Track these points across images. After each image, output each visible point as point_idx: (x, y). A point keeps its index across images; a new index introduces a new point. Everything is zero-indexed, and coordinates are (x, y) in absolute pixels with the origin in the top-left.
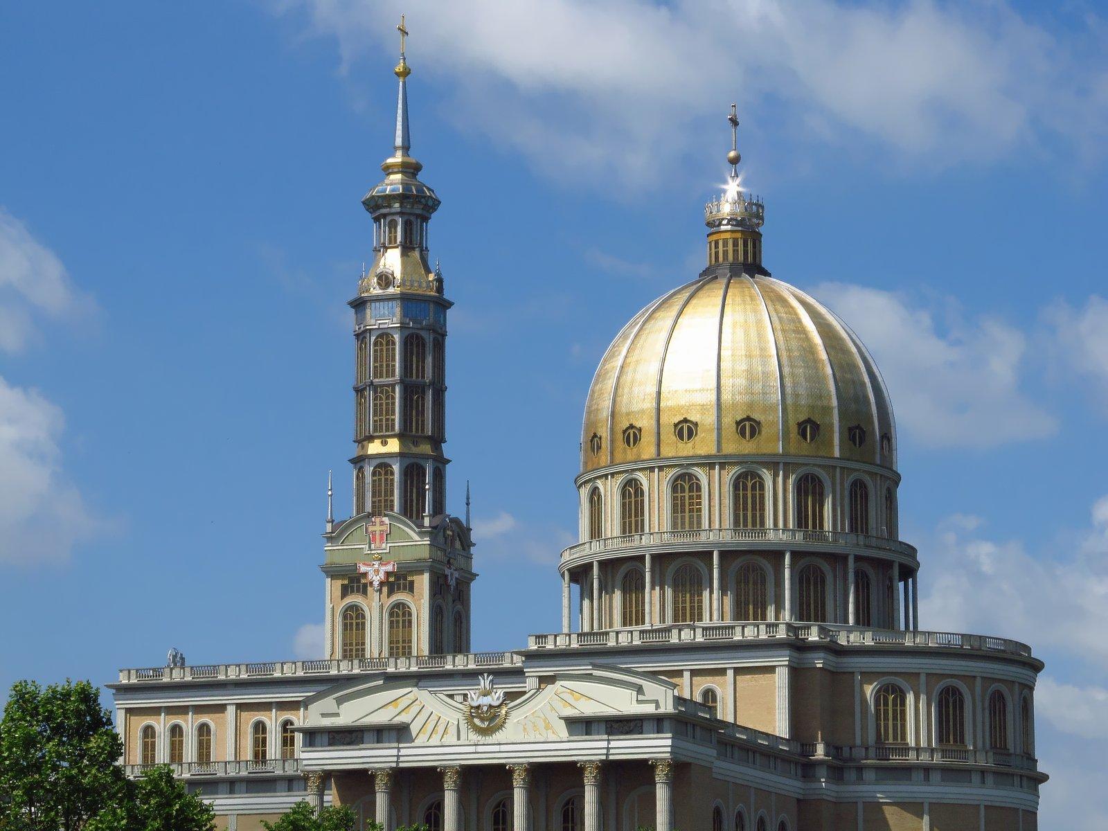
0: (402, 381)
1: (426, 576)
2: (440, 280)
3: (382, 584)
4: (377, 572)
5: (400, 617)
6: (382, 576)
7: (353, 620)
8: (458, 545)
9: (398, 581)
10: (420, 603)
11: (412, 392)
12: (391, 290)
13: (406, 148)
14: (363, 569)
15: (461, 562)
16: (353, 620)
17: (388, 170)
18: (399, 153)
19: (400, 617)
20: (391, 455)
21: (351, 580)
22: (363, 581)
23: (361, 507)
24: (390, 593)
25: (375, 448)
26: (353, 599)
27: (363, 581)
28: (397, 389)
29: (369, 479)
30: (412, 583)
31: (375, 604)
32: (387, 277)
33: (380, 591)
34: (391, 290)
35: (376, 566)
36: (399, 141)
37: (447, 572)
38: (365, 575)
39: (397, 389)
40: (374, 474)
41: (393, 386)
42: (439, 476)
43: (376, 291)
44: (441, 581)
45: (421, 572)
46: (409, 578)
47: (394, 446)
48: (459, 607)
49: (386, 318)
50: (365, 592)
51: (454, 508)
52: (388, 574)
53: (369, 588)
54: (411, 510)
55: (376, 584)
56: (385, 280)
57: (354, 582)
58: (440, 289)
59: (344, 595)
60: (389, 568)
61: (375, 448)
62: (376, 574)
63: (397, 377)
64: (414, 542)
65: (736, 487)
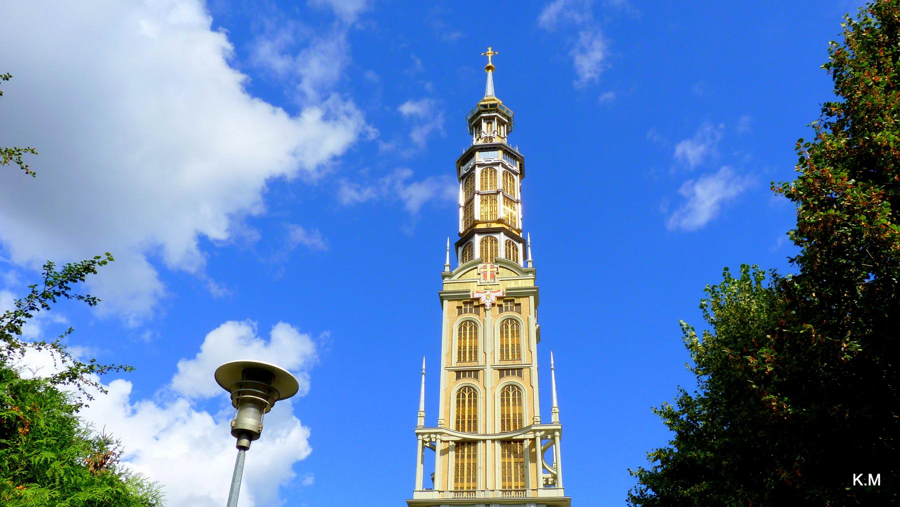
3: (493, 305)
5: (510, 326)
6: (494, 300)
14: (476, 296)
16: (469, 328)
21: (465, 303)
24: (501, 311)
27: (476, 304)
35: (488, 293)
38: (478, 299)
46: (517, 301)
50: (478, 313)
52: (499, 298)
59: (460, 313)
60: (500, 294)
62: (488, 298)
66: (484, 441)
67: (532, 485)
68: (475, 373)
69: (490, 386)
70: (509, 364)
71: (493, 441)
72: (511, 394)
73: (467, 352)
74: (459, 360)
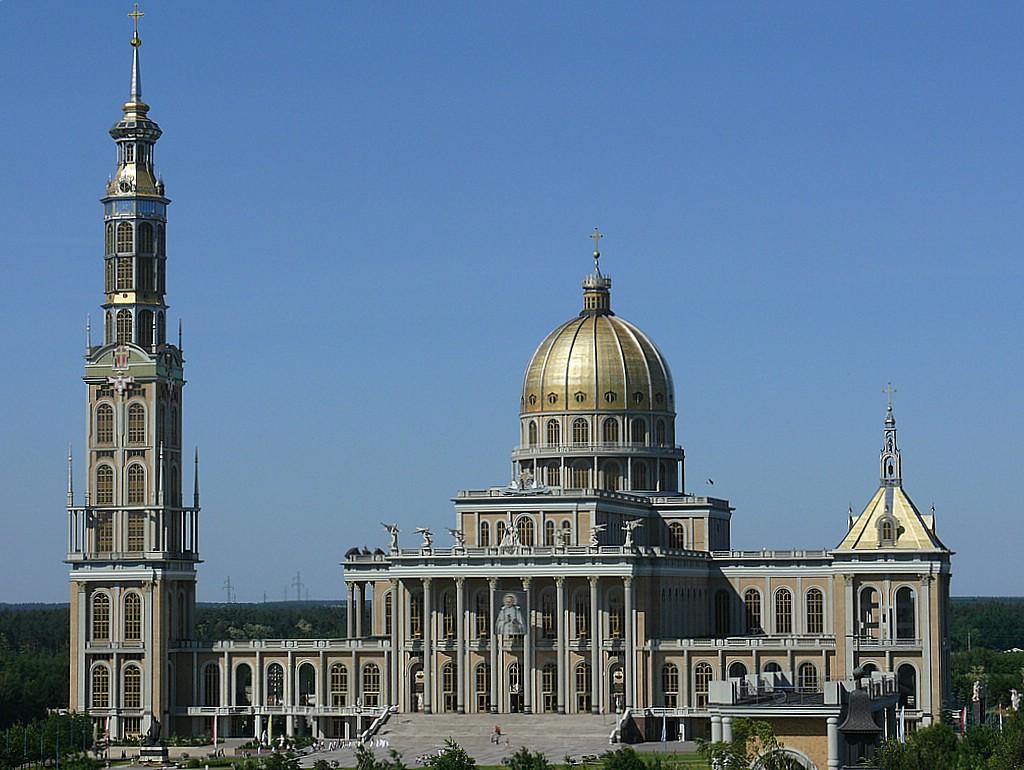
0: (136, 255)
1: (154, 384)
2: (162, 186)
3: (124, 391)
4: (120, 382)
5: (135, 413)
7: (105, 414)
8: (174, 362)
9: (134, 389)
10: (150, 403)
11: (144, 264)
12: (129, 194)
13: (138, 95)
14: (111, 381)
15: (175, 374)
16: (105, 414)
17: (126, 110)
18: (134, 99)
19: (135, 413)
20: (130, 305)
22: (111, 388)
23: (109, 338)
25: (119, 299)
26: (104, 400)
28: (134, 259)
29: (115, 320)
30: (144, 390)
31: (120, 403)
32: (127, 185)
33: (123, 395)
34: (129, 194)
36: (134, 90)
37: (168, 382)
38: (112, 384)
39: (134, 259)
40: (118, 317)
41: (131, 257)
42: (162, 317)
43: (121, 194)
44: (164, 387)
45: (150, 382)
47: (132, 298)
48: (175, 404)
49: (128, 213)
51: (171, 339)
52: (128, 384)
53: (115, 392)
54: (144, 342)
55: (120, 390)
56: (125, 186)
57: (105, 389)
58: (162, 193)
60: (129, 380)
61: (119, 299)
63: (134, 252)
64: (145, 362)
65: (605, 425)
66: (117, 511)
67: (146, 549)
68: (111, 454)
69: (118, 465)
70: (135, 446)
71: (123, 511)
72: (136, 474)
73: (105, 435)
74: (99, 441)
